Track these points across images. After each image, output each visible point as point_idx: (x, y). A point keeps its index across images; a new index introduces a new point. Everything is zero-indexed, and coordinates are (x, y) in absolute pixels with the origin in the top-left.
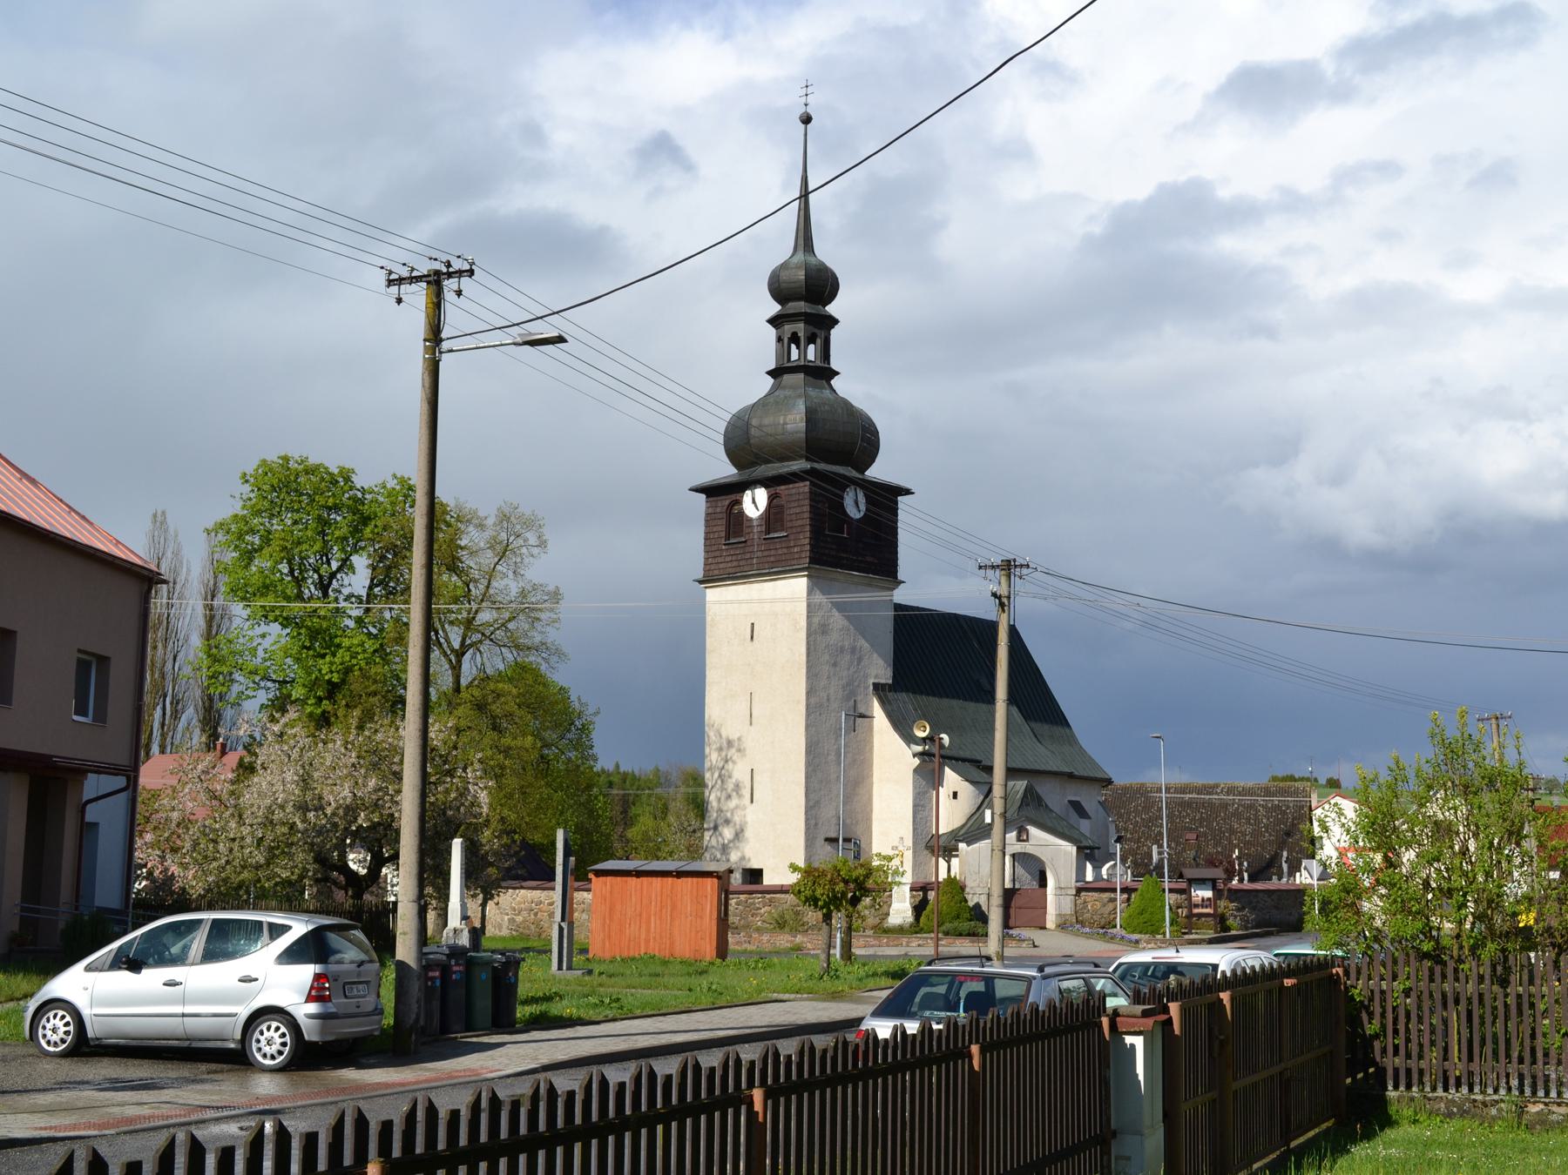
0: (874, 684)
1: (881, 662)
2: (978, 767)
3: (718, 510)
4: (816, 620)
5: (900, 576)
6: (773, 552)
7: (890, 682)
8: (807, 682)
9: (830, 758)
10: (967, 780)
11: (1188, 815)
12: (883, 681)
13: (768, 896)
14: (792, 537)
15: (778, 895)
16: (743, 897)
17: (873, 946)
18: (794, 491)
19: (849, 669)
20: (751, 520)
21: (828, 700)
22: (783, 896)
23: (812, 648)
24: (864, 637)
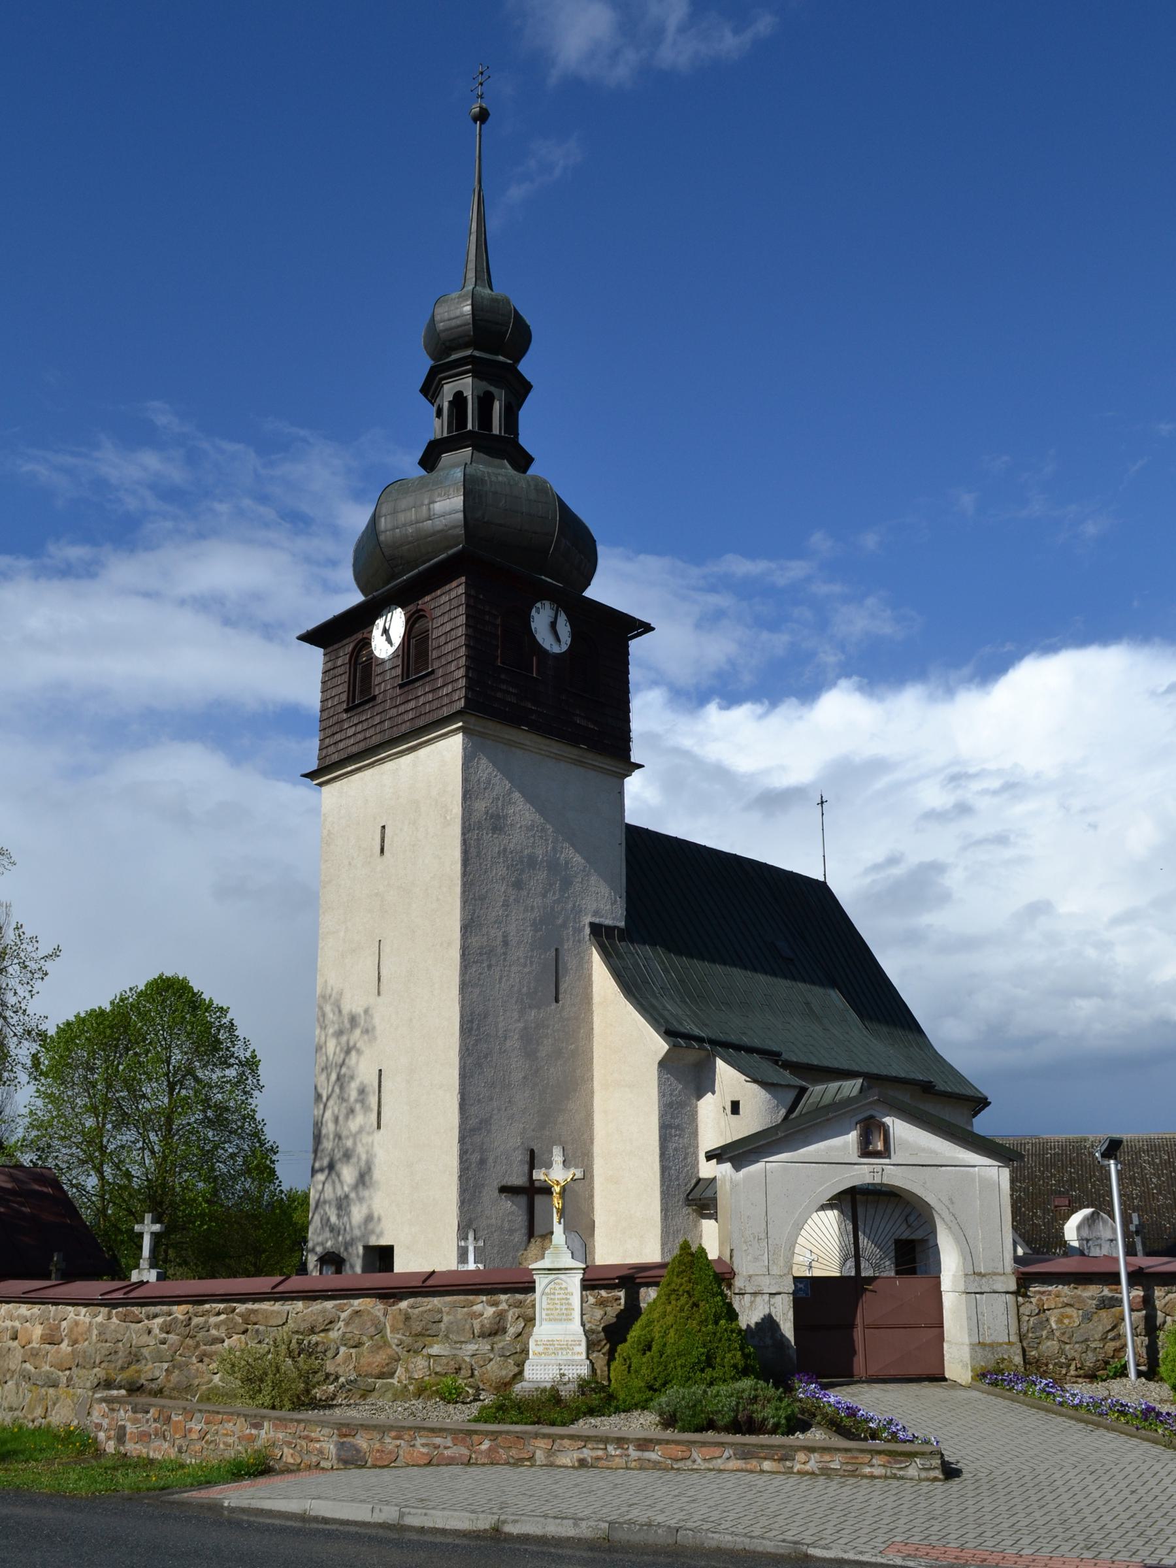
0: (593, 926)
1: (604, 890)
2: (776, 1063)
3: (339, 662)
4: (480, 806)
5: (635, 758)
6: (412, 704)
7: (622, 924)
8: (463, 908)
9: (508, 1043)
10: (755, 1081)
11: (1053, 1175)
12: (608, 922)
13: (241, 1308)
14: (440, 672)
15: (265, 1306)
16: (179, 1311)
17: (450, 1462)
18: (445, 598)
19: (544, 896)
20: (383, 662)
21: (506, 943)
22: (277, 1306)
23: (473, 851)
24: (573, 845)
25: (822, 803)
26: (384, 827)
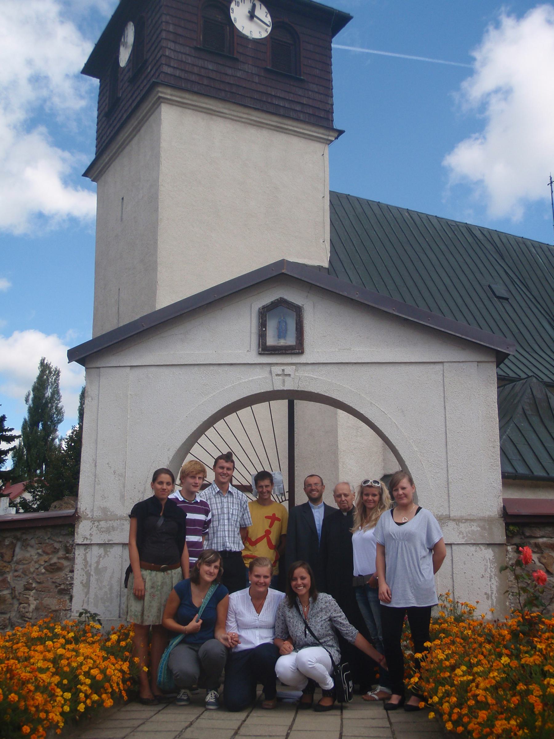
7: (326, 264)
25: (551, 183)
26: (123, 199)
